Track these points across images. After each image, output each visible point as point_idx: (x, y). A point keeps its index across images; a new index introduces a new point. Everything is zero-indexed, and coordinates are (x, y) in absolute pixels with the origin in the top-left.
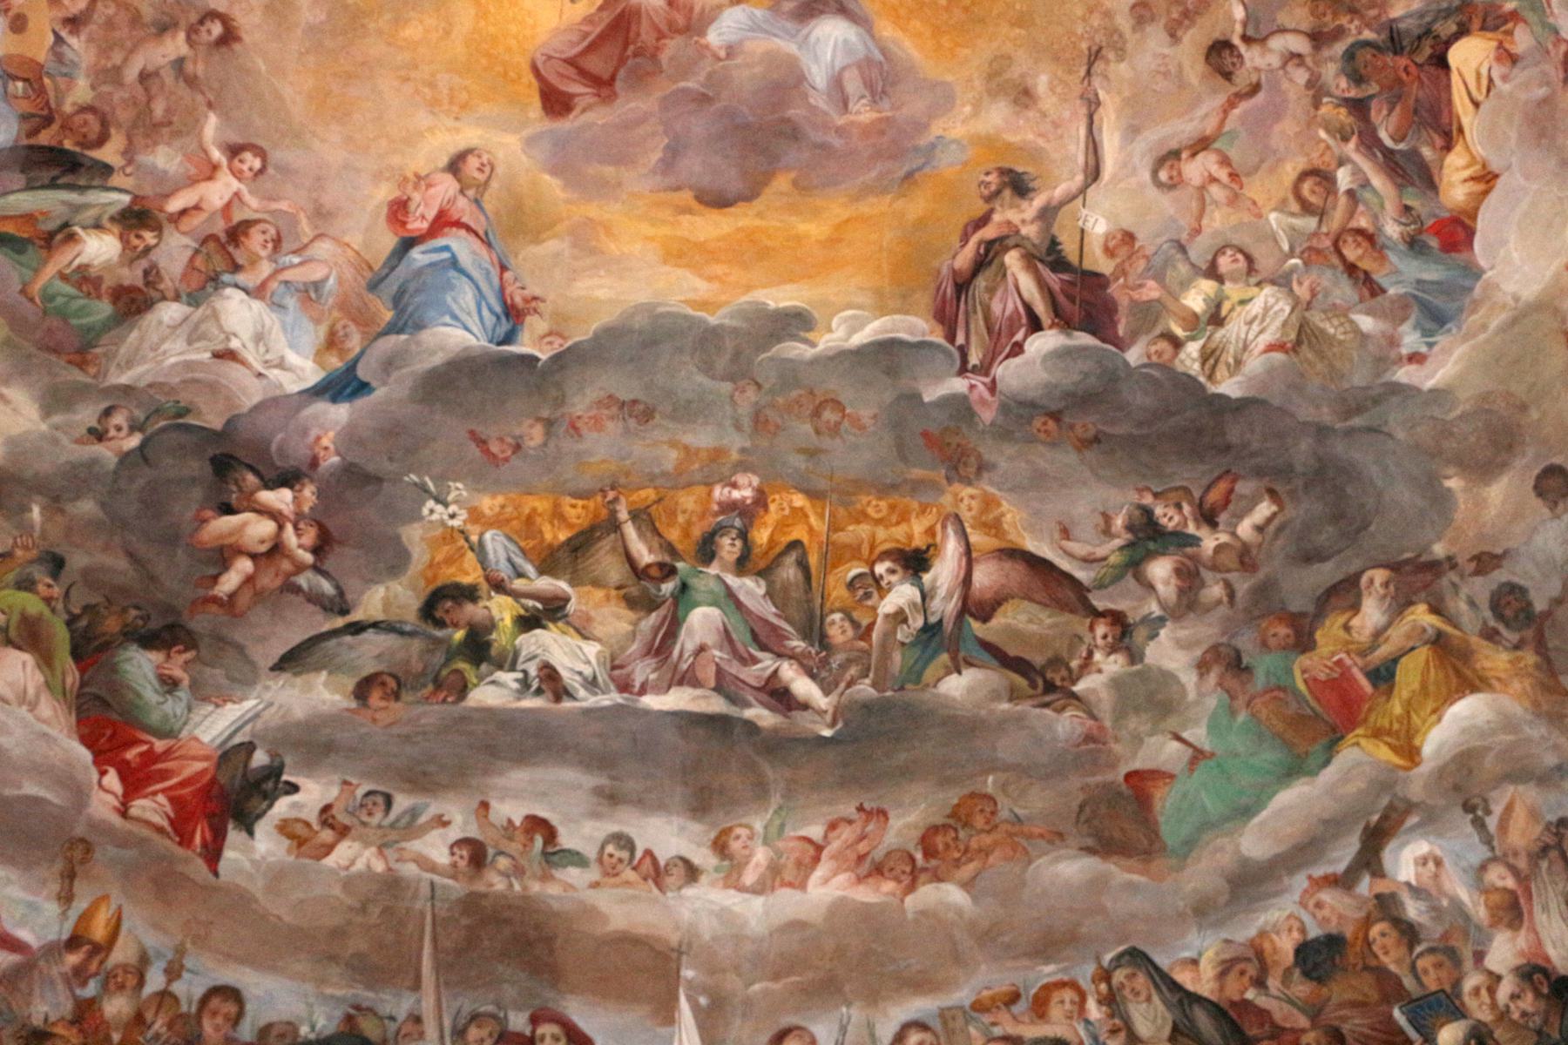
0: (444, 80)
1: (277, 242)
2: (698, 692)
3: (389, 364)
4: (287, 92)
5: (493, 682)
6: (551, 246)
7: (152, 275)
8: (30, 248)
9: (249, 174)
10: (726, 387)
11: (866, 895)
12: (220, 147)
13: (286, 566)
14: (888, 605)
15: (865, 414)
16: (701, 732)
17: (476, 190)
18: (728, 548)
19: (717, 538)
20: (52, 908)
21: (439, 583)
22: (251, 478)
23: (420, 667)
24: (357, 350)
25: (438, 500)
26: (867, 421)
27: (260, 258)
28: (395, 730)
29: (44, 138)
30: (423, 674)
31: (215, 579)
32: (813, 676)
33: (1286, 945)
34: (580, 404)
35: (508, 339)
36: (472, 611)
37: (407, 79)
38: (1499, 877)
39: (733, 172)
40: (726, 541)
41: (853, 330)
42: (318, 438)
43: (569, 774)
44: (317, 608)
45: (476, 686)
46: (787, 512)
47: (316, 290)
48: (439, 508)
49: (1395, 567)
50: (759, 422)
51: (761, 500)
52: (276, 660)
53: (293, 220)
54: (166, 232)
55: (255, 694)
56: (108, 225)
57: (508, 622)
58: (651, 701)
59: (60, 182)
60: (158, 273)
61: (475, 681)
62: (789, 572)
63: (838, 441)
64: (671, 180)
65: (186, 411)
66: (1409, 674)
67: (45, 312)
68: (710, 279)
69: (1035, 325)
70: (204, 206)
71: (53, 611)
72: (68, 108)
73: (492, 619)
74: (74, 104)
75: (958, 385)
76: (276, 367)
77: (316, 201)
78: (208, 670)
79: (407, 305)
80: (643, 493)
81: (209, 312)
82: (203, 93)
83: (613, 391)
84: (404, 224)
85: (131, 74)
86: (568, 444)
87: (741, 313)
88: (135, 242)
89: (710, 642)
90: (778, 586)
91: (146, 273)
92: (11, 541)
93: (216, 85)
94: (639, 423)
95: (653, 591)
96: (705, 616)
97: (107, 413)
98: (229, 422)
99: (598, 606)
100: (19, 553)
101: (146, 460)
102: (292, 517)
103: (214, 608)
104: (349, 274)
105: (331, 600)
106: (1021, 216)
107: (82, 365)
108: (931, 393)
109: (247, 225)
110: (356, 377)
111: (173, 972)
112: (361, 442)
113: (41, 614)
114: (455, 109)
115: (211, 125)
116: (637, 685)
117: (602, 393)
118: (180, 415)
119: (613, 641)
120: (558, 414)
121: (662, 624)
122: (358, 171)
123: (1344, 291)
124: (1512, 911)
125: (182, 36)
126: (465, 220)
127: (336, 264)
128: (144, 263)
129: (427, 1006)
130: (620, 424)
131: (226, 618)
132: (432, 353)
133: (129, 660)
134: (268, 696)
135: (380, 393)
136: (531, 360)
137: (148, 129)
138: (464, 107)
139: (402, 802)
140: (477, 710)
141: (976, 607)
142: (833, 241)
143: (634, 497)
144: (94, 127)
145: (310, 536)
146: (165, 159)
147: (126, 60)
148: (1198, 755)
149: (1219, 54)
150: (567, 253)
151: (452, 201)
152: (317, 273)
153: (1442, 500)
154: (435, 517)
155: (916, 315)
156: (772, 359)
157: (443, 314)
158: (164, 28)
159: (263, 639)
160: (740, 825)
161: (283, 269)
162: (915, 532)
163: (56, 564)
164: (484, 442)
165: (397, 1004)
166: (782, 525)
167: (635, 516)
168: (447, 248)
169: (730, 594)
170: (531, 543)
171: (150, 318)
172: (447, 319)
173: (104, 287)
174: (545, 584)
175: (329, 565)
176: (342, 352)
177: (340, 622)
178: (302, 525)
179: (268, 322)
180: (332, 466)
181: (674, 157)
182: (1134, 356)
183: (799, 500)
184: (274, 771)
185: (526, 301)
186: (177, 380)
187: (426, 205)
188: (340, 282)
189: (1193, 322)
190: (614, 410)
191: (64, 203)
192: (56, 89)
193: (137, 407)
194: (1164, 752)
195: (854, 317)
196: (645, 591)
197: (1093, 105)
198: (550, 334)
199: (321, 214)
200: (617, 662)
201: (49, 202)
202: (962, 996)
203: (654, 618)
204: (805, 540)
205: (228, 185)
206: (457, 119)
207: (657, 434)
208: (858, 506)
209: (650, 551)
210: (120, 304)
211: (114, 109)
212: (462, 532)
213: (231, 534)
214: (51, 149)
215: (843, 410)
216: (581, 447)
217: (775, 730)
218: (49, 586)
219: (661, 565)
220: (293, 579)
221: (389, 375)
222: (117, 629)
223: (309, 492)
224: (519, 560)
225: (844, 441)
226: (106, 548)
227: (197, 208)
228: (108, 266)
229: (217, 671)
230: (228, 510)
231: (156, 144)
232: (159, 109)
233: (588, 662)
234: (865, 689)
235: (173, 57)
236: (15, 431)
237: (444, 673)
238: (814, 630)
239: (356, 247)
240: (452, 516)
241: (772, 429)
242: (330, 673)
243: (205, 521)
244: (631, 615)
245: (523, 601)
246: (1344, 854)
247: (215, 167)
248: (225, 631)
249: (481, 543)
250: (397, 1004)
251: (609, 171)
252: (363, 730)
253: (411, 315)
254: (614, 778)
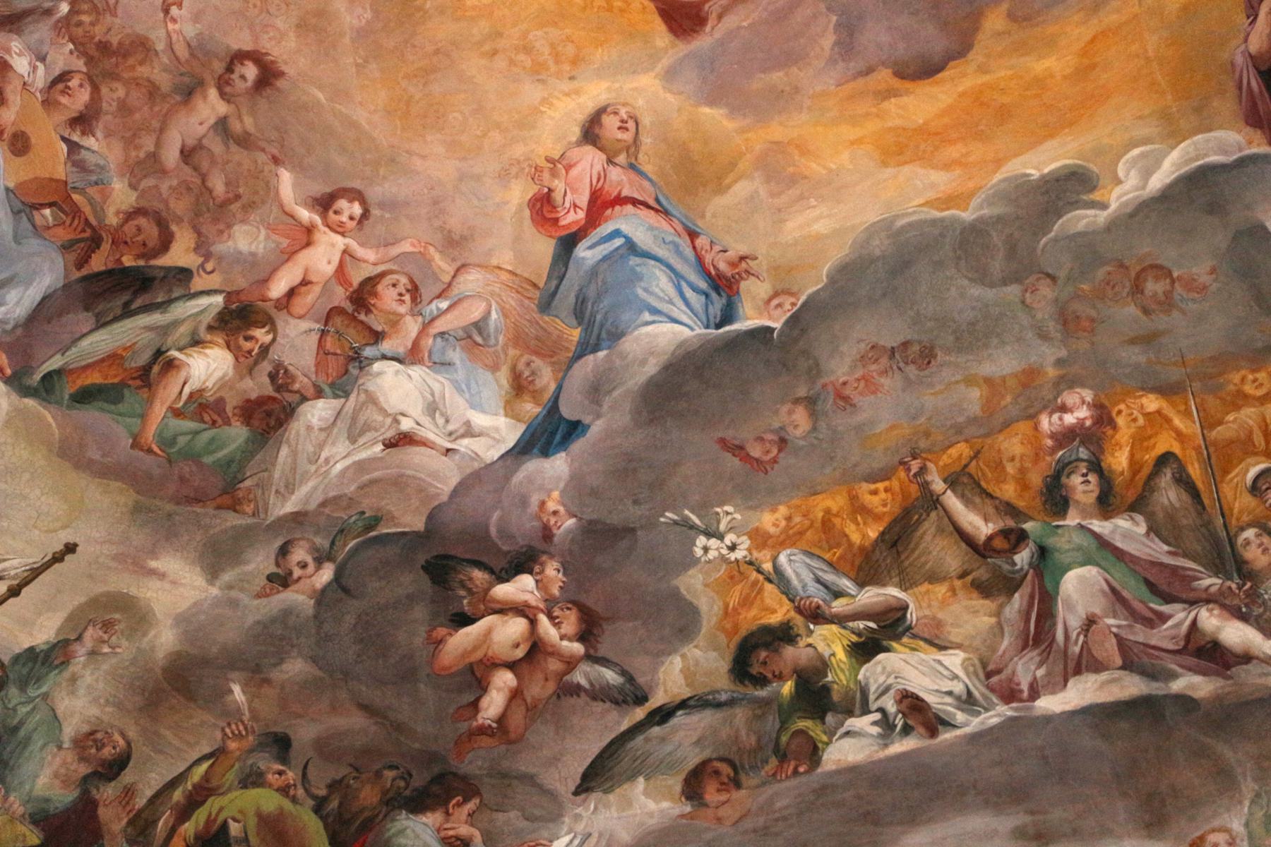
0: (540, 40)
1: (414, 290)
2: (1104, 676)
3: (596, 391)
4: (360, 115)
5: (847, 734)
6: (741, 189)
7: (280, 377)
8: (126, 392)
9: (351, 225)
10: (1013, 290)
12: (305, 205)
13: (554, 665)
15: (1201, 271)
16: (1124, 725)
18: (1081, 488)
19: (1064, 480)
21: (743, 632)
22: (479, 575)
23: (753, 739)
24: (553, 387)
25: (709, 535)
26: (1205, 279)
27: (402, 316)
28: (748, 824)
29: (98, 263)
30: (759, 747)
31: (475, 706)
32: (1244, 618)
34: (840, 369)
35: (728, 316)
36: (793, 654)
37: (495, 53)
39: (930, 30)
40: (1076, 480)
41: (1147, 174)
42: (543, 504)
43: (977, 822)
44: (608, 704)
45: (827, 744)
46: (1141, 421)
47: (480, 333)
48: (713, 543)
50: (1068, 322)
51: (1103, 417)
52: (578, 781)
53: (422, 258)
54: (280, 324)
55: (565, 829)
56: (209, 337)
57: (841, 655)
58: (1050, 704)
59: (133, 307)
60: (286, 371)
61: (825, 738)
62: (1169, 495)
63: (1175, 314)
64: (856, 65)
65: (375, 521)
67: (170, 462)
68: (947, 167)
70: (313, 278)
71: (294, 800)
72: (112, 220)
73: (821, 657)
74: (118, 213)
76: (463, 436)
77: (441, 229)
78: (500, 817)
79: (593, 315)
80: (953, 452)
81: (363, 397)
82: (263, 150)
83: (874, 339)
84: (557, 220)
85: (171, 156)
86: (842, 421)
87: (1000, 196)
88: (247, 345)
89: (1097, 611)
90: (1161, 515)
91: (273, 377)
92: (219, 735)
93: (274, 135)
94: (920, 368)
95: (1006, 567)
96: (1082, 579)
97: (284, 551)
98: (431, 517)
99: (944, 603)
100: (232, 745)
101: (346, 590)
102: (542, 606)
103: (485, 741)
104: (512, 301)
105: (620, 689)
107: (234, 507)
109: (371, 283)
110: (561, 417)
112: (594, 493)
113: (281, 809)
114: (567, 67)
115: (286, 182)
116: (1025, 687)
117: (862, 345)
118: (370, 528)
119: (977, 643)
120: (818, 386)
121: (1031, 605)
122: (478, 178)
125: (213, 93)
126: (626, 192)
127: (492, 294)
128: (266, 367)
130: (898, 376)
131: (503, 747)
132: (644, 362)
133: (401, 832)
134: (580, 827)
135: (597, 428)
138: (575, 61)
140: (838, 772)
142: (1084, 71)
143: (945, 459)
144: (151, 231)
145: (571, 622)
147: (158, 144)
150: (763, 193)
151: (602, 176)
152: (474, 312)
154: (712, 554)
155: (1221, 127)
156: (1056, 240)
157: (641, 312)
158: (189, 92)
159: (555, 760)
160: (1213, 831)
161: (433, 320)
163: (281, 745)
164: (741, 448)
166: (1140, 440)
167: (953, 482)
168: (617, 233)
169: (1103, 543)
170: (839, 552)
171: (296, 427)
172: (647, 316)
173: (229, 409)
174: (871, 596)
175: (603, 650)
176: (535, 395)
177: (640, 713)
178: (557, 612)
179: (437, 387)
180: (569, 531)
181: (851, 35)
183: (1152, 403)
185: (733, 265)
186: (353, 488)
187: (574, 191)
188: (504, 313)
190: (884, 361)
191: (149, 328)
192: (91, 201)
193: (317, 533)
195: (1143, 156)
196: (996, 571)
198: (776, 294)
199: (453, 243)
200: (991, 667)
203: (1018, 600)
204: (1176, 449)
205: (333, 245)
206: (572, 78)
207: (947, 374)
208: (1232, 387)
209: (986, 520)
210: (256, 423)
211: (166, 203)
212: (750, 563)
213: (475, 648)
214: (110, 273)
215: (1170, 274)
216: (860, 418)
217: (1218, 699)
218: (280, 773)
219: (1005, 533)
220: (567, 678)
221: (601, 406)
222: (375, 800)
223: (552, 570)
224: (830, 577)
225: (1183, 312)
226: (334, 709)
227: (305, 282)
228: (223, 384)
229: (513, 814)
230: (465, 620)
231: (229, 226)
232: (218, 185)
233: (955, 677)
235: (212, 121)
236: (184, 606)
237: (784, 739)
239: (510, 268)
240: (733, 548)
241: (1086, 324)
242: (647, 779)
243: (440, 642)
244: (988, 605)
245: (851, 624)
247: (309, 230)
248: (505, 764)
249: (776, 568)
251: (777, 77)
252: (708, 836)
253: (602, 326)
254: (1032, 813)
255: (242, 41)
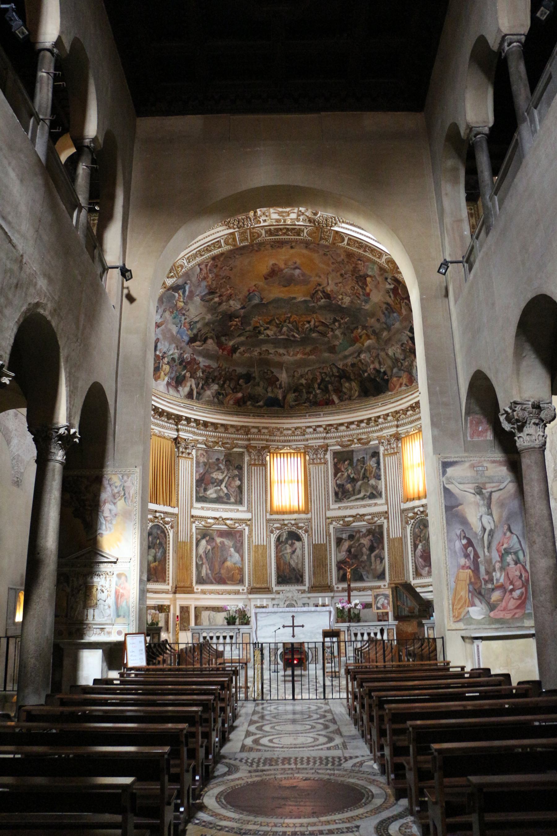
11: (303, 357)
14: (306, 327)
17: (257, 288)
20: (216, 364)
33: (350, 364)
38: (372, 358)
49: (362, 326)
51: (291, 316)
66: (364, 337)
69: (322, 299)
75: (313, 304)
106: (320, 288)
108: (310, 305)
111: (229, 369)
123: (356, 298)
124: (373, 362)
129: (256, 370)
135: (247, 308)
136: (264, 304)
137: (221, 287)
139: (252, 349)
141: (316, 327)
146: (223, 290)
148: (341, 344)
149: (342, 275)
153: (367, 320)
158: (223, 278)
162: (309, 319)
163: (214, 330)
165: (252, 370)
182: (333, 302)
184: (238, 347)
189: (340, 299)
194: (337, 343)
197: (328, 279)
201: (211, 297)
202: (315, 367)
223: (240, 319)
234: (303, 335)
238: (297, 329)
246: (356, 355)
250: (252, 370)
255: (228, 275)
